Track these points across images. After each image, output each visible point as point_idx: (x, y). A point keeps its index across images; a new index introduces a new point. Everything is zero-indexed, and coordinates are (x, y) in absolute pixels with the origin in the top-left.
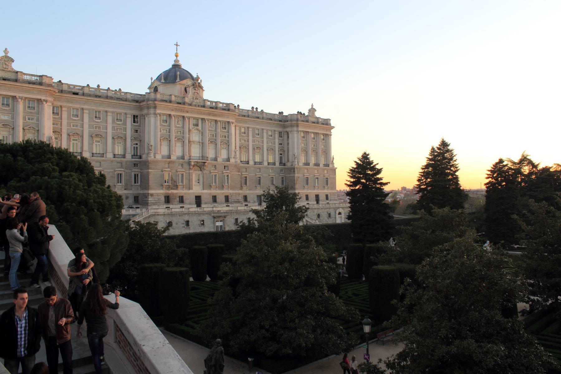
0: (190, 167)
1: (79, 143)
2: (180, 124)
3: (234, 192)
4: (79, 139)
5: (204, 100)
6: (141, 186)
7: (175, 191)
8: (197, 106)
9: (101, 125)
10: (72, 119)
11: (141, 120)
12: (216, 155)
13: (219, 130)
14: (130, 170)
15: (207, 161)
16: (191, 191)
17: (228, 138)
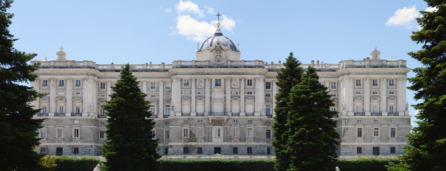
0: (209, 122)
2: (202, 85)
3: (258, 144)
7: (193, 144)
8: (219, 67)
12: (240, 111)
15: (227, 116)
16: (209, 143)
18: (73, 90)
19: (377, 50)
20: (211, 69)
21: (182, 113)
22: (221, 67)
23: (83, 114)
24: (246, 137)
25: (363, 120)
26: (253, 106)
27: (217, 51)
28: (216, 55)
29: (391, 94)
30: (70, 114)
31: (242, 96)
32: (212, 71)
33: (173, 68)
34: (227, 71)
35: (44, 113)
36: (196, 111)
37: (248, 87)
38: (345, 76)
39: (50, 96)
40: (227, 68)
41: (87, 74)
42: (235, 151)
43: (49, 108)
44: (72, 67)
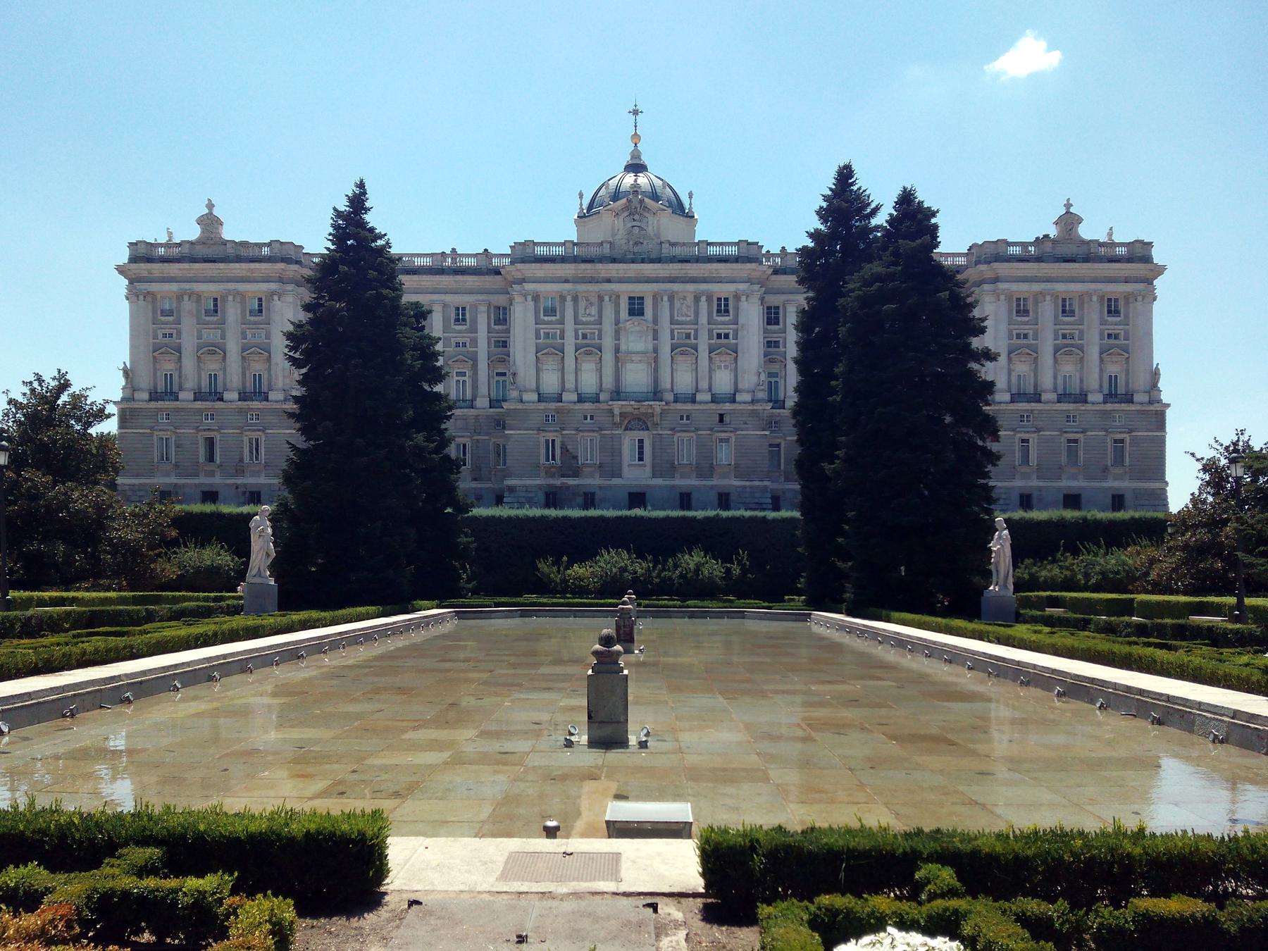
2: (593, 314)
8: (640, 261)
12: (697, 388)
13: (703, 319)
17: (736, 338)
18: (244, 326)
19: (1072, 210)
20: (616, 266)
21: (539, 394)
22: (643, 261)
23: (272, 396)
24: (715, 463)
25: (1036, 415)
26: (733, 374)
27: (634, 215)
28: (630, 225)
29: (1112, 341)
30: (235, 396)
31: (703, 344)
32: (620, 272)
33: (512, 263)
34: (661, 272)
35: (166, 393)
36: (576, 387)
37: (720, 319)
38: (986, 287)
40: (659, 262)
41: (281, 280)
42: (685, 500)
43: (180, 377)
44: (238, 259)
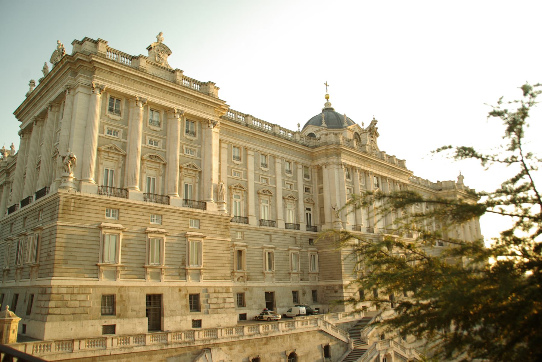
1: (243, 202)
4: (242, 196)
5: (381, 152)
6: (318, 274)
9: (268, 176)
10: (233, 162)
11: (313, 173)
14: (306, 248)
39: (126, 143)
